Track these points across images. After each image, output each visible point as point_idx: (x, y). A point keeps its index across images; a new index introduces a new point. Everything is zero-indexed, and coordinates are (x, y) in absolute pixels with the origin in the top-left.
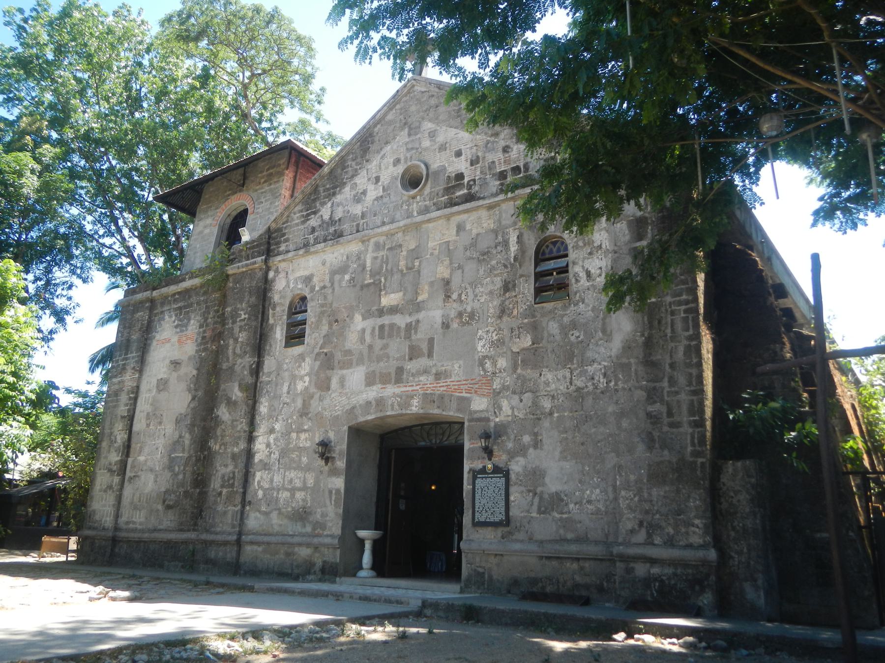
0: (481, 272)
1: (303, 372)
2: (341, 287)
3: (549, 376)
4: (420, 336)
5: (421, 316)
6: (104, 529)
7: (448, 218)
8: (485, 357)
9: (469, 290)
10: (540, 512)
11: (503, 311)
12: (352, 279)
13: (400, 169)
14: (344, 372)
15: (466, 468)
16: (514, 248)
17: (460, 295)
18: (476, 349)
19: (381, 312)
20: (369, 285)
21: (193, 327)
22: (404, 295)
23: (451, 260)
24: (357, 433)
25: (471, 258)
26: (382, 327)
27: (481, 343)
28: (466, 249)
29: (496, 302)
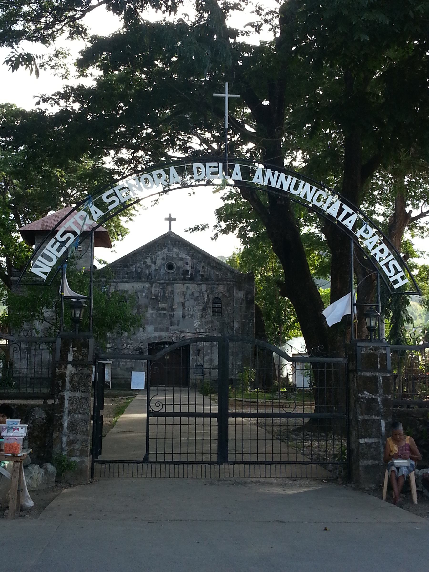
0: (195, 303)
4: (175, 319)
5: (175, 312)
8: (197, 328)
11: (202, 316)
12: (146, 296)
13: (164, 262)
15: (191, 357)
16: (206, 299)
17: (188, 309)
19: (159, 309)
20: (154, 299)
23: (185, 297)
24: (150, 345)
27: (195, 324)
28: (190, 295)
29: (201, 313)
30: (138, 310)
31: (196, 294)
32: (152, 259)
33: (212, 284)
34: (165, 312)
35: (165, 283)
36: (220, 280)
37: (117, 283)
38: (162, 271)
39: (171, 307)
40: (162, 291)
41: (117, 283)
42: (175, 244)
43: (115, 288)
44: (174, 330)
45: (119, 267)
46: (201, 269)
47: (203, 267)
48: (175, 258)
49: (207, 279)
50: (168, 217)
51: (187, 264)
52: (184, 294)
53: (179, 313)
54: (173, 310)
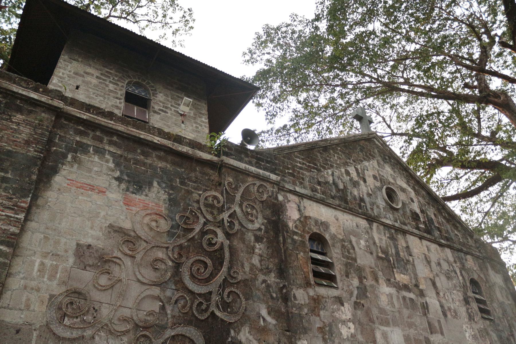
1: (344, 317)
2: (361, 249)
14: (385, 328)
16: (461, 278)
17: (444, 294)
22: (411, 279)
26: (404, 298)
45: (300, 163)
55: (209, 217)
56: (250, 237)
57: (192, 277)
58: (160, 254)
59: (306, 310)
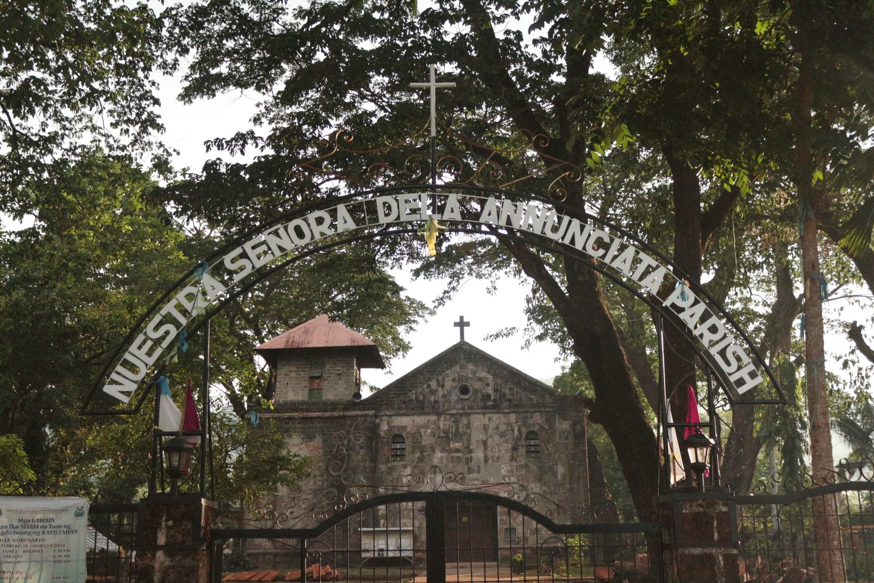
0: (502, 440)
1: (406, 474)
3: (533, 486)
4: (472, 464)
5: (473, 455)
6: (264, 549)
7: (484, 414)
9: (497, 448)
10: (530, 534)
11: (513, 459)
12: (432, 432)
13: (455, 384)
15: (499, 519)
16: (516, 433)
17: (492, 449)
18: (501, 472)
19: (450, 451)
20: (442, 437)
21: (318, 441)
25: (496, 434)
26: (452, 457)
28: (493, 429)
29: (509, 454)
30: (421, 453)
31: (503, 428)
32: (438, 381)
33: (524, 412)
34: (460, 455)
35: (458, 414)
36: (536, 407)
37: (391, 416)
38: (454, 398)
39: (467, 448)
40: (454, 425)
41: (391, 416)
42: (470, 358)
43: (388, 424)
44: (474, 480)
46: (507, 391)
47: (511, 389)
48: (471, 378)
49: (516, 406)
50: (458, 320)
51: (488, 385)
52: (485, 428)
53: (479, 454)
54: (470, 451)
55: (340, 443)
56: (358, 447)
57: (333, 470)
58: (321, 464)
59: (385, 474)
